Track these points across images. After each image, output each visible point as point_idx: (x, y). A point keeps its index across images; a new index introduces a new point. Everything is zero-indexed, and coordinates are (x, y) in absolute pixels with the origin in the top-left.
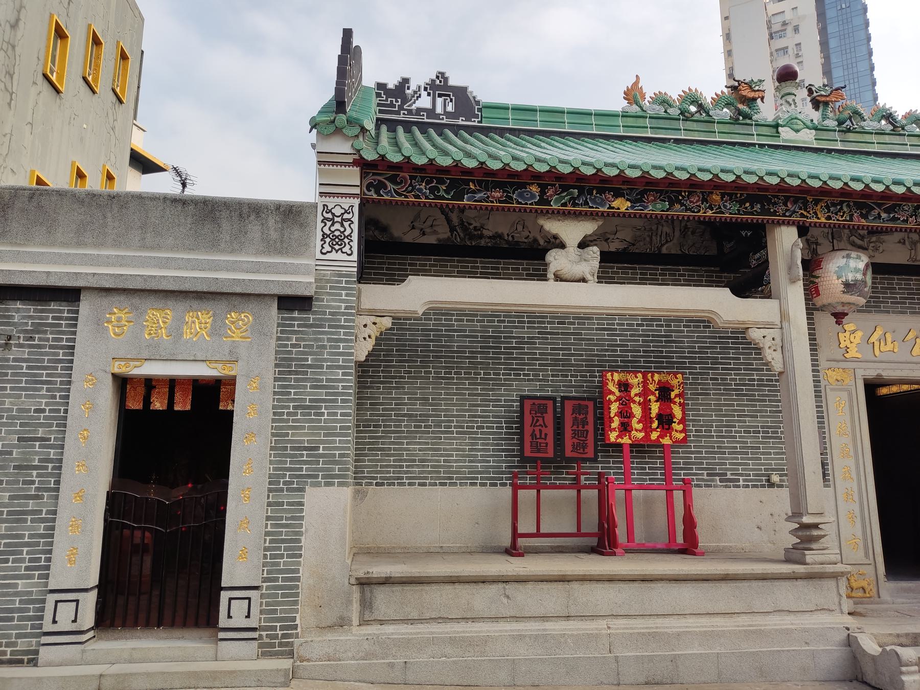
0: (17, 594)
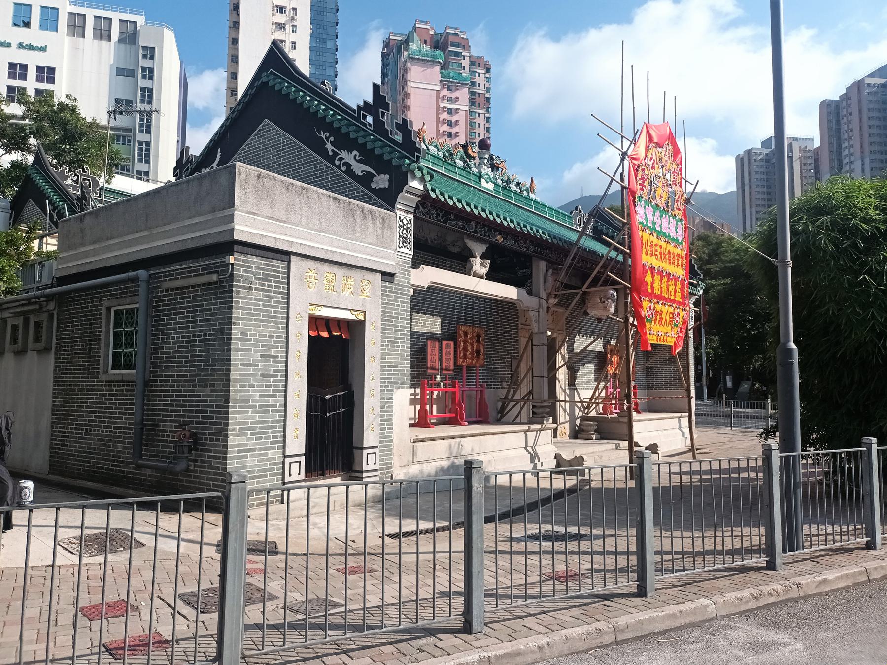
0: (268, 460)
